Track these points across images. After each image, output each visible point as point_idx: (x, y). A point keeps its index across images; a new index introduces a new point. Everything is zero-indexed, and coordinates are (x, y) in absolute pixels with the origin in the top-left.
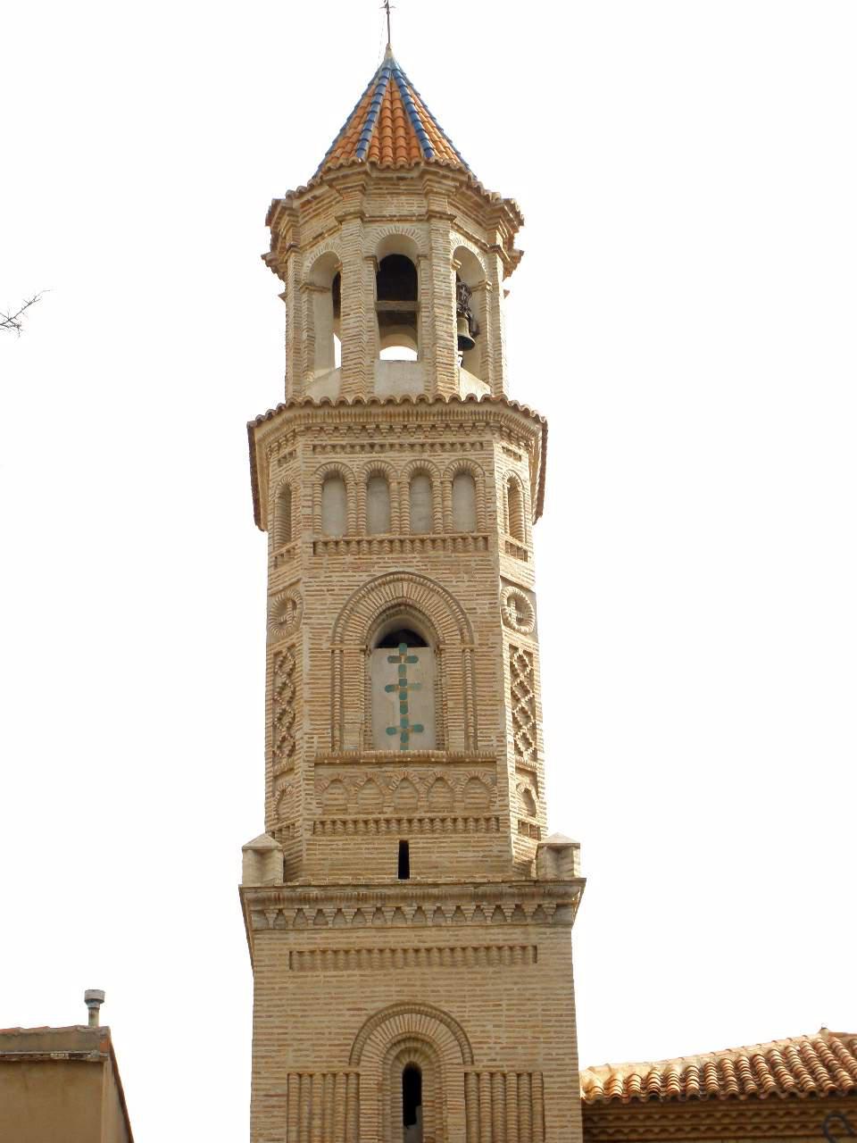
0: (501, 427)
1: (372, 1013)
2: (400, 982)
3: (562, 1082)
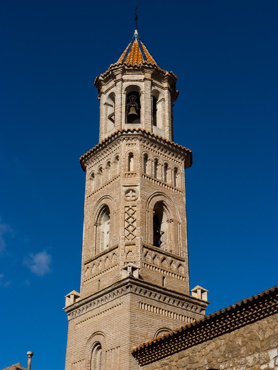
1: (88, 338)
2: (95, 326)
3: (125, 347)
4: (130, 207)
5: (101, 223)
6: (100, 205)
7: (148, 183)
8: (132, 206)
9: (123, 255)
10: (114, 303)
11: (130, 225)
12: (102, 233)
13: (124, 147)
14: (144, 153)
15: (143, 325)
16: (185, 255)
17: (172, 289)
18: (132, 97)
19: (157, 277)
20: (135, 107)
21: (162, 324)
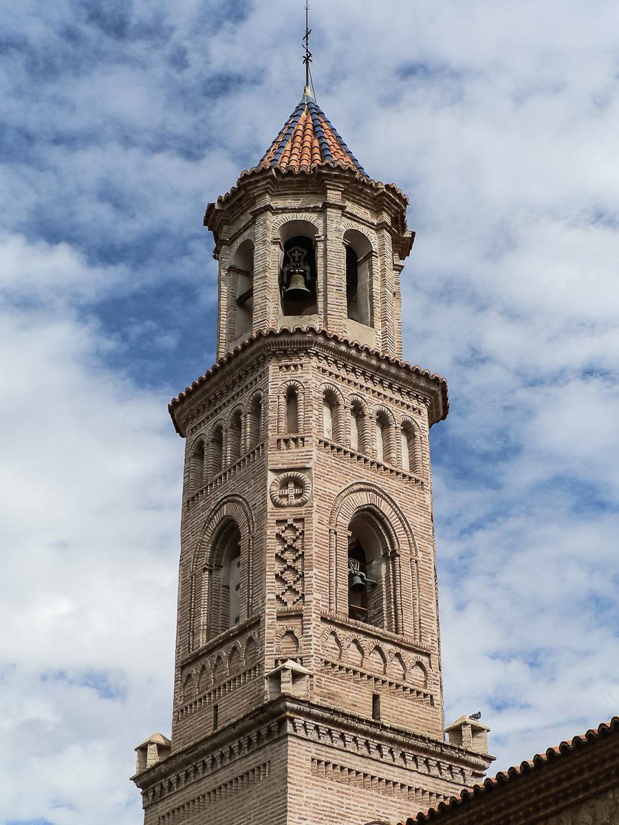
0: (274, 352)
5: (222, 564)
6: (217, 519)
7: (333, 461)
8: (296, 520)
9: (272, 643)
10: (250, 763)
11: (289, 567)
12: (225, 589)
13: (274, 372)
14: (323, 387)
15: (321, 816)
16: (429, 639)
17: (395, 726)
18: (294, 252)
19: (358, 696)
20: (304, 274)
21: (369, 813)
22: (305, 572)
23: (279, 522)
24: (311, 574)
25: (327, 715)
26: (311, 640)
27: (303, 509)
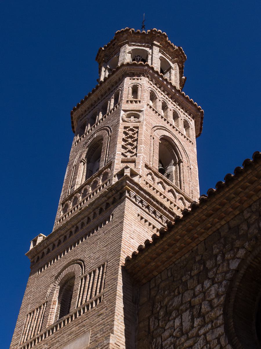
4: (131, 127)
22: (138, 145)
23: (125, 128)
24: (141, 146)
25: (147, 197)
26: (139, 170)
27: (138, 124)
